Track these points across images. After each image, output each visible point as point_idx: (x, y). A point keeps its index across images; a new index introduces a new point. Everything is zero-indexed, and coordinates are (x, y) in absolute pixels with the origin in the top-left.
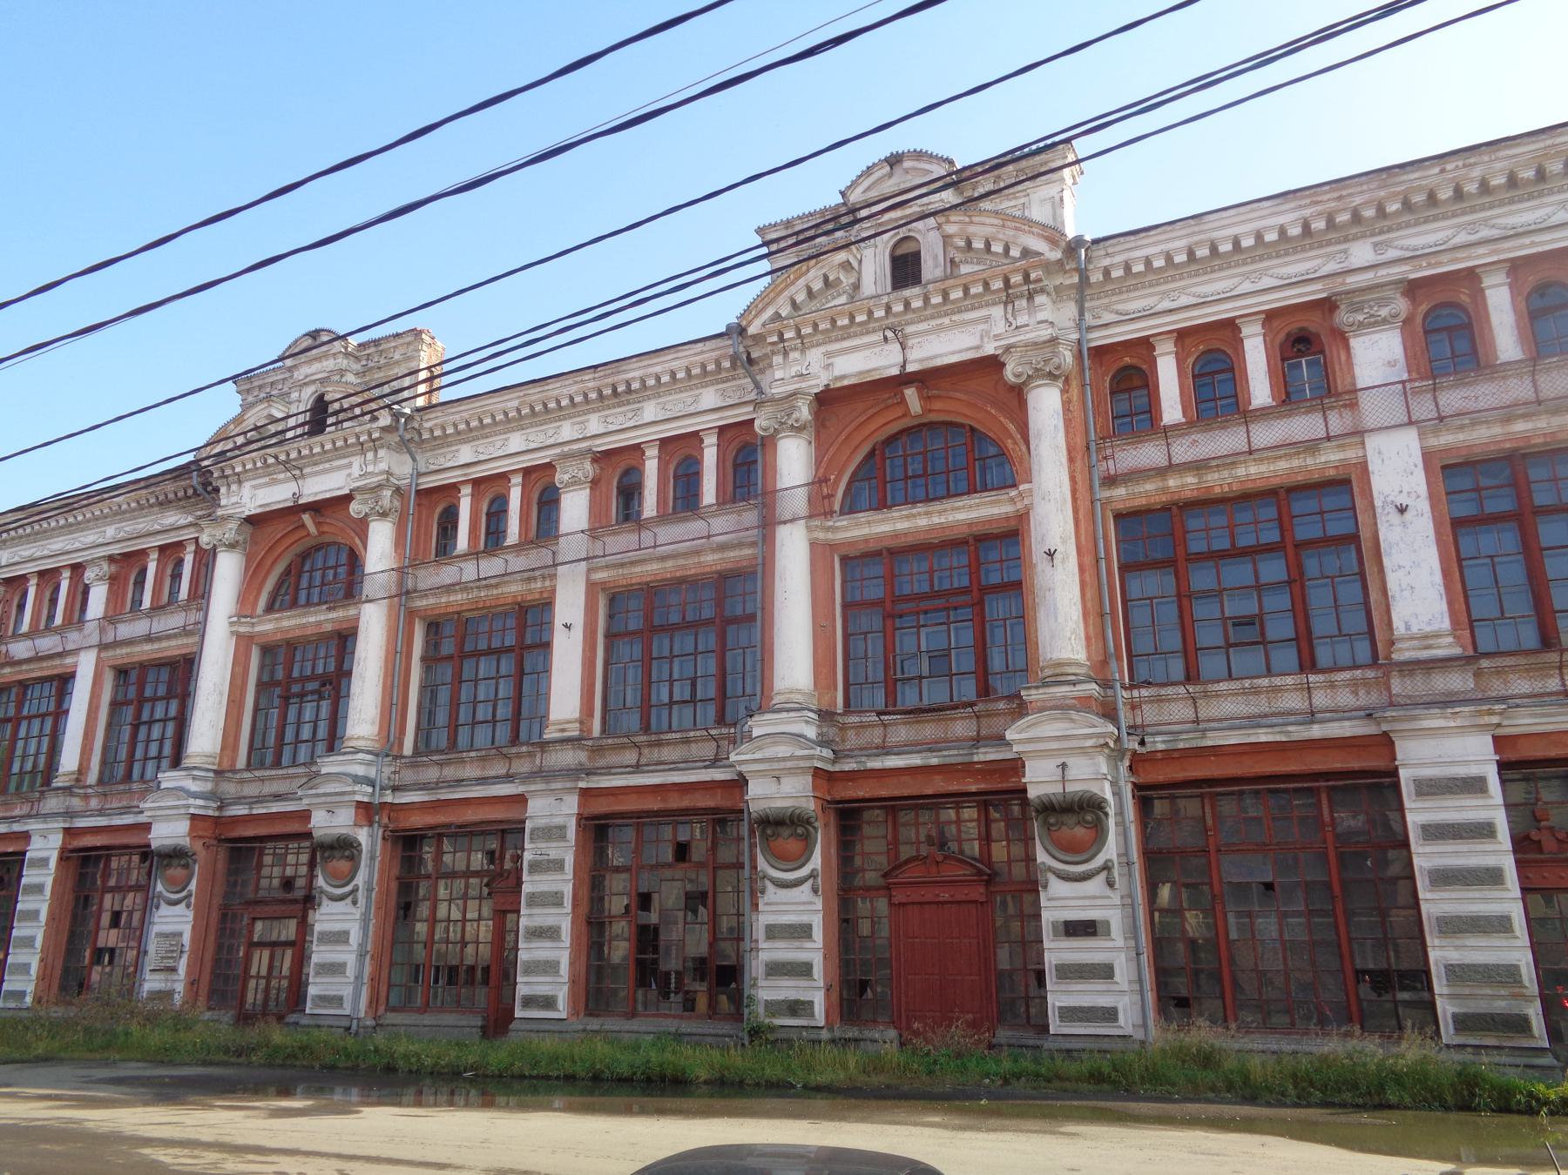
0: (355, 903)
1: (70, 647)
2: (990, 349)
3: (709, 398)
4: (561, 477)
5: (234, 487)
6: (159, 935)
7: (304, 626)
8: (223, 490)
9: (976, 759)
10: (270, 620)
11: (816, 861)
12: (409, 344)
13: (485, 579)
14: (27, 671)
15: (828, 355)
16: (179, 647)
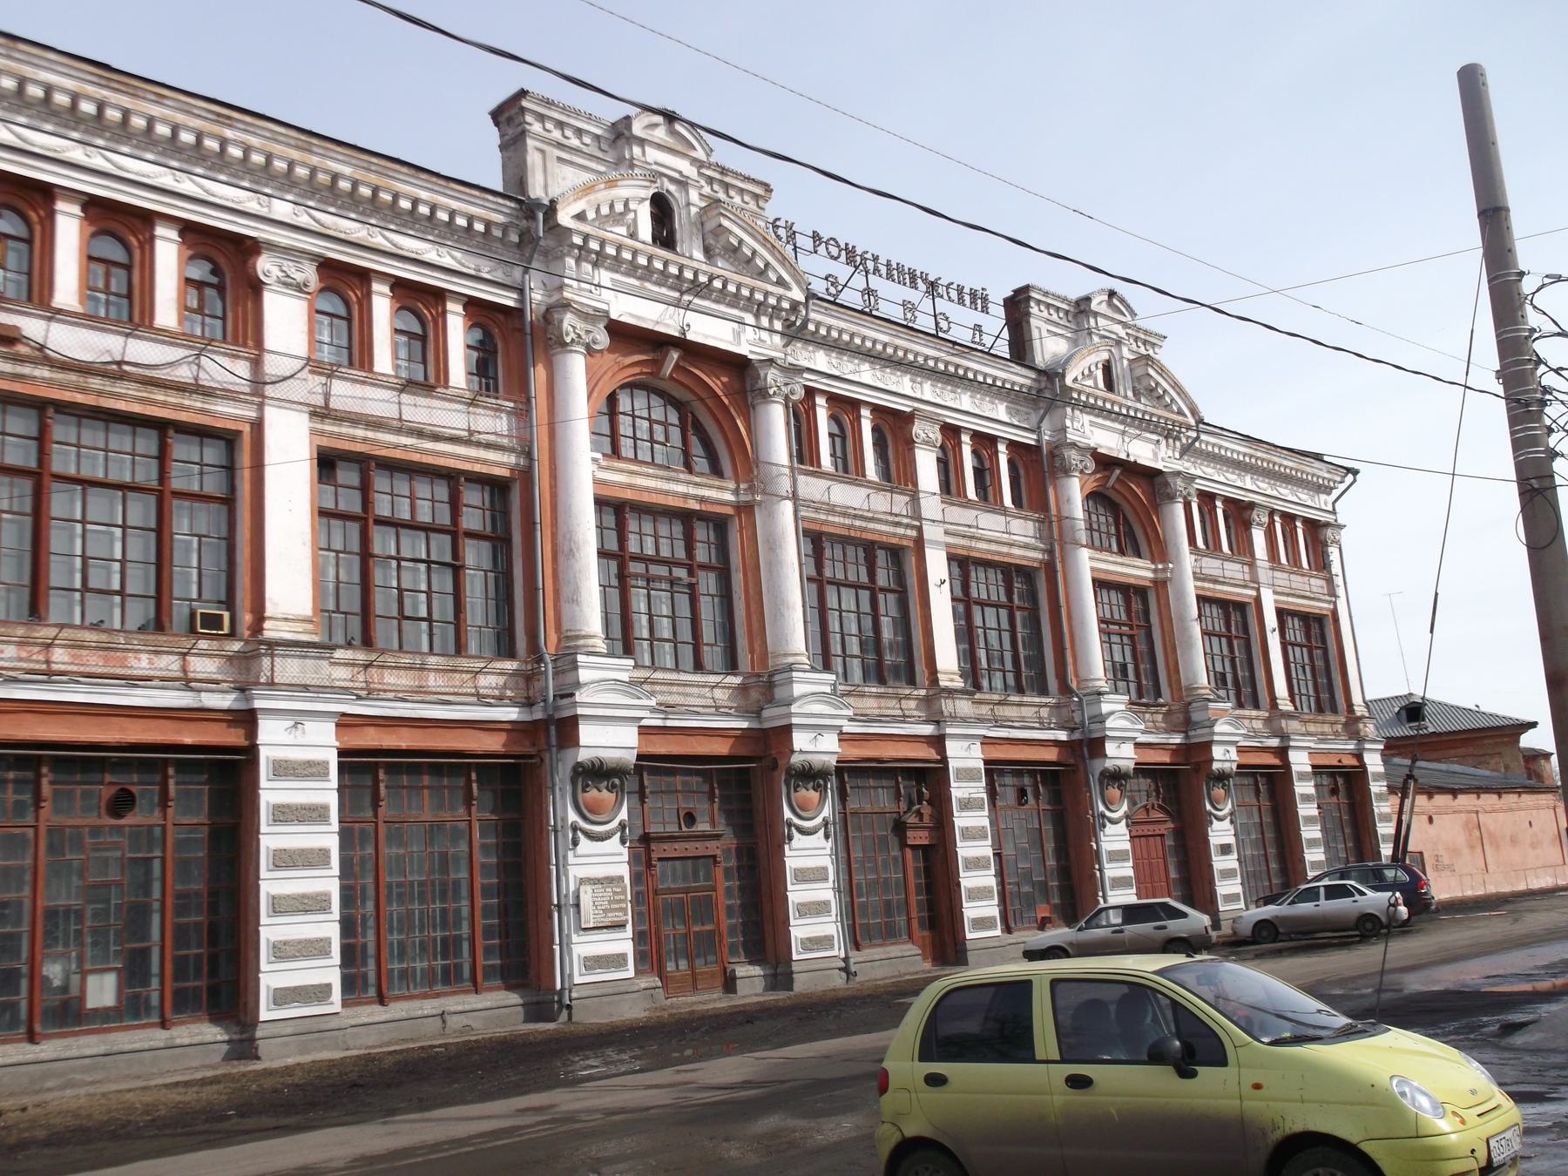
0: (827, 837)
1: (205, 380)
2: (1159, 465)
3: (1001, 411)
4: (919, 429)
5: (587, 267)
6: (583, 881)
7: (666, 493)
8: (570, 262)
9: (1171, 741)
10: (622, 471)
11: (1125, 808)
12: (756, 197)
13: (896, 515)
14: (100, 393)
15: (1092, 424)
16: (468, 459)
